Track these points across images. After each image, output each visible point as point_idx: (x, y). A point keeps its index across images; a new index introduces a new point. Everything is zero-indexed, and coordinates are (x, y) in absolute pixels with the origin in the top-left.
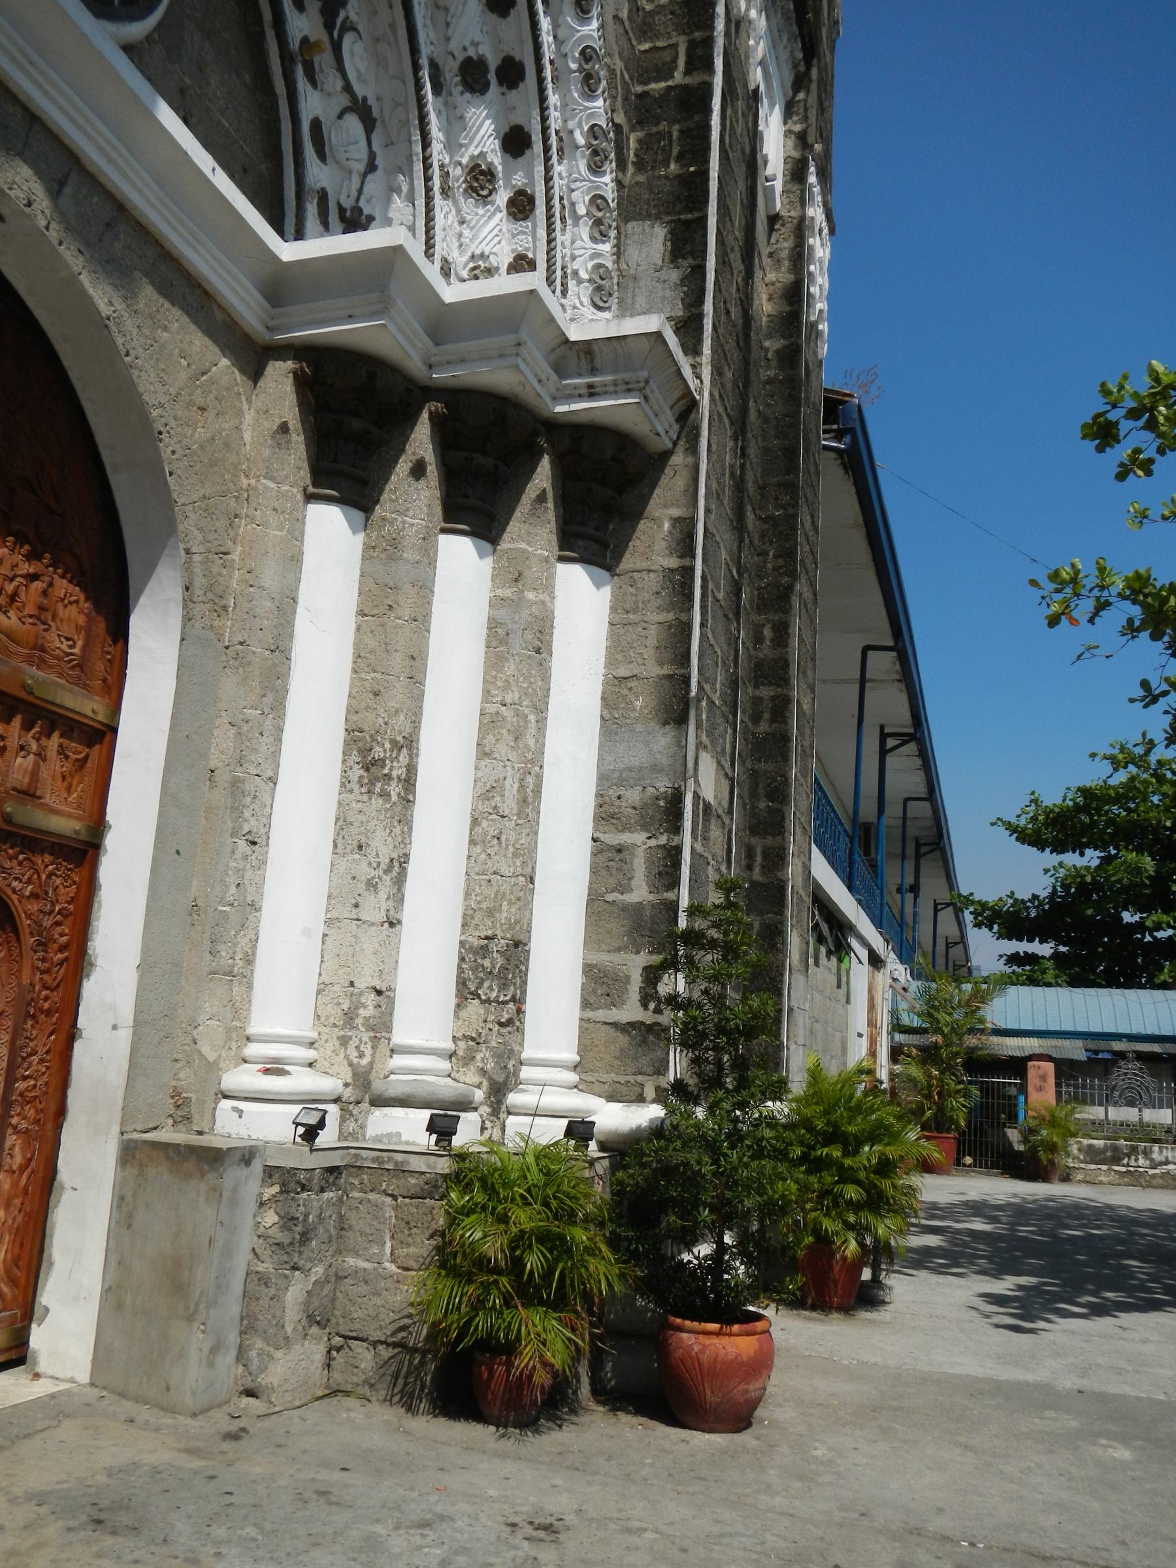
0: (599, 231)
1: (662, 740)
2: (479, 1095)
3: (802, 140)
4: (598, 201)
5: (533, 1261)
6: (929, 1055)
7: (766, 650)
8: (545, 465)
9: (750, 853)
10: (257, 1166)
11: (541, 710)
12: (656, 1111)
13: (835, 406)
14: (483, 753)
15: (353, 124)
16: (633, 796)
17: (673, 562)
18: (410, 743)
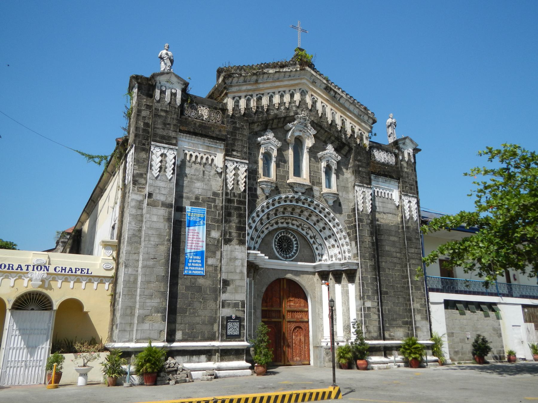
0: (347, 245)
1: (360, 301)
2: (345, 341)
10: (323, 348)
14: (343, 306)
15: (320, 246)
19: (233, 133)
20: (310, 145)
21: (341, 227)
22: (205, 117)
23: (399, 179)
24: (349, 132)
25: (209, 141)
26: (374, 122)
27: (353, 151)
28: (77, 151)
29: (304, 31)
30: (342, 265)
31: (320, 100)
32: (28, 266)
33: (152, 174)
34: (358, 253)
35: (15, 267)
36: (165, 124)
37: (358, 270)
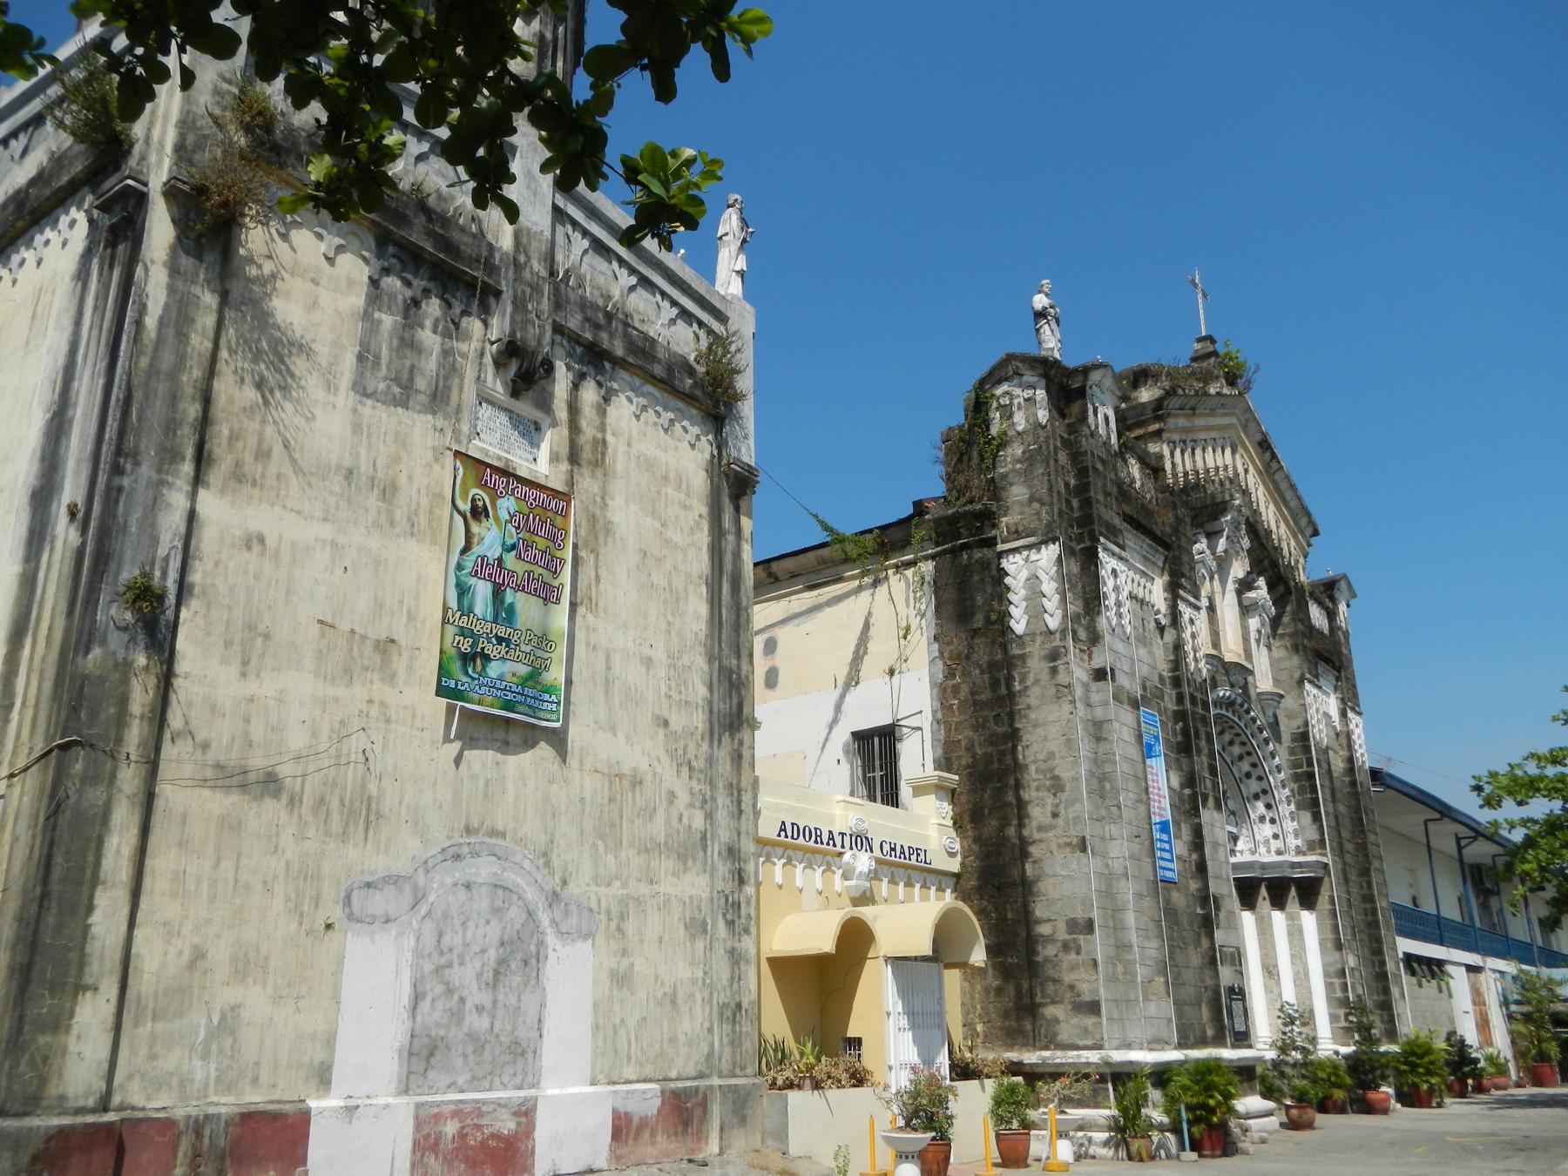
0: (1293, 819)
1: (1337, 954)
3: (1343, 700)
4: (1291, 813)
5: (1333, 1079)
6: (1528, 1018)
7: (1365, 891)
8: (1293, 889)
9: (1373, 963)
11: (1304, 950)
12: (1354, 1048)
13: (1376, 775)
14: (1293, 964)
16: (1332, 969)
17: (1330, 907)
18: (1276, 966)
19: (1176, 530)
20: (1241, 575)
21: (1282, 776)
22: (1138, 485)
23: (1339, 671)
24: (1285, 552)
25: (1149, 545)
26: (1316, 533)
27: (1293, 597)
28: (816, 516)
29: (1205, 296)
30: (1293, 865)
31: (1251, 469)
32: (843, 834)
33: (1107, 618)
34: (1322, 841)
35: (825, 839)
36: (1107, 494)
37: (1326, 879)
